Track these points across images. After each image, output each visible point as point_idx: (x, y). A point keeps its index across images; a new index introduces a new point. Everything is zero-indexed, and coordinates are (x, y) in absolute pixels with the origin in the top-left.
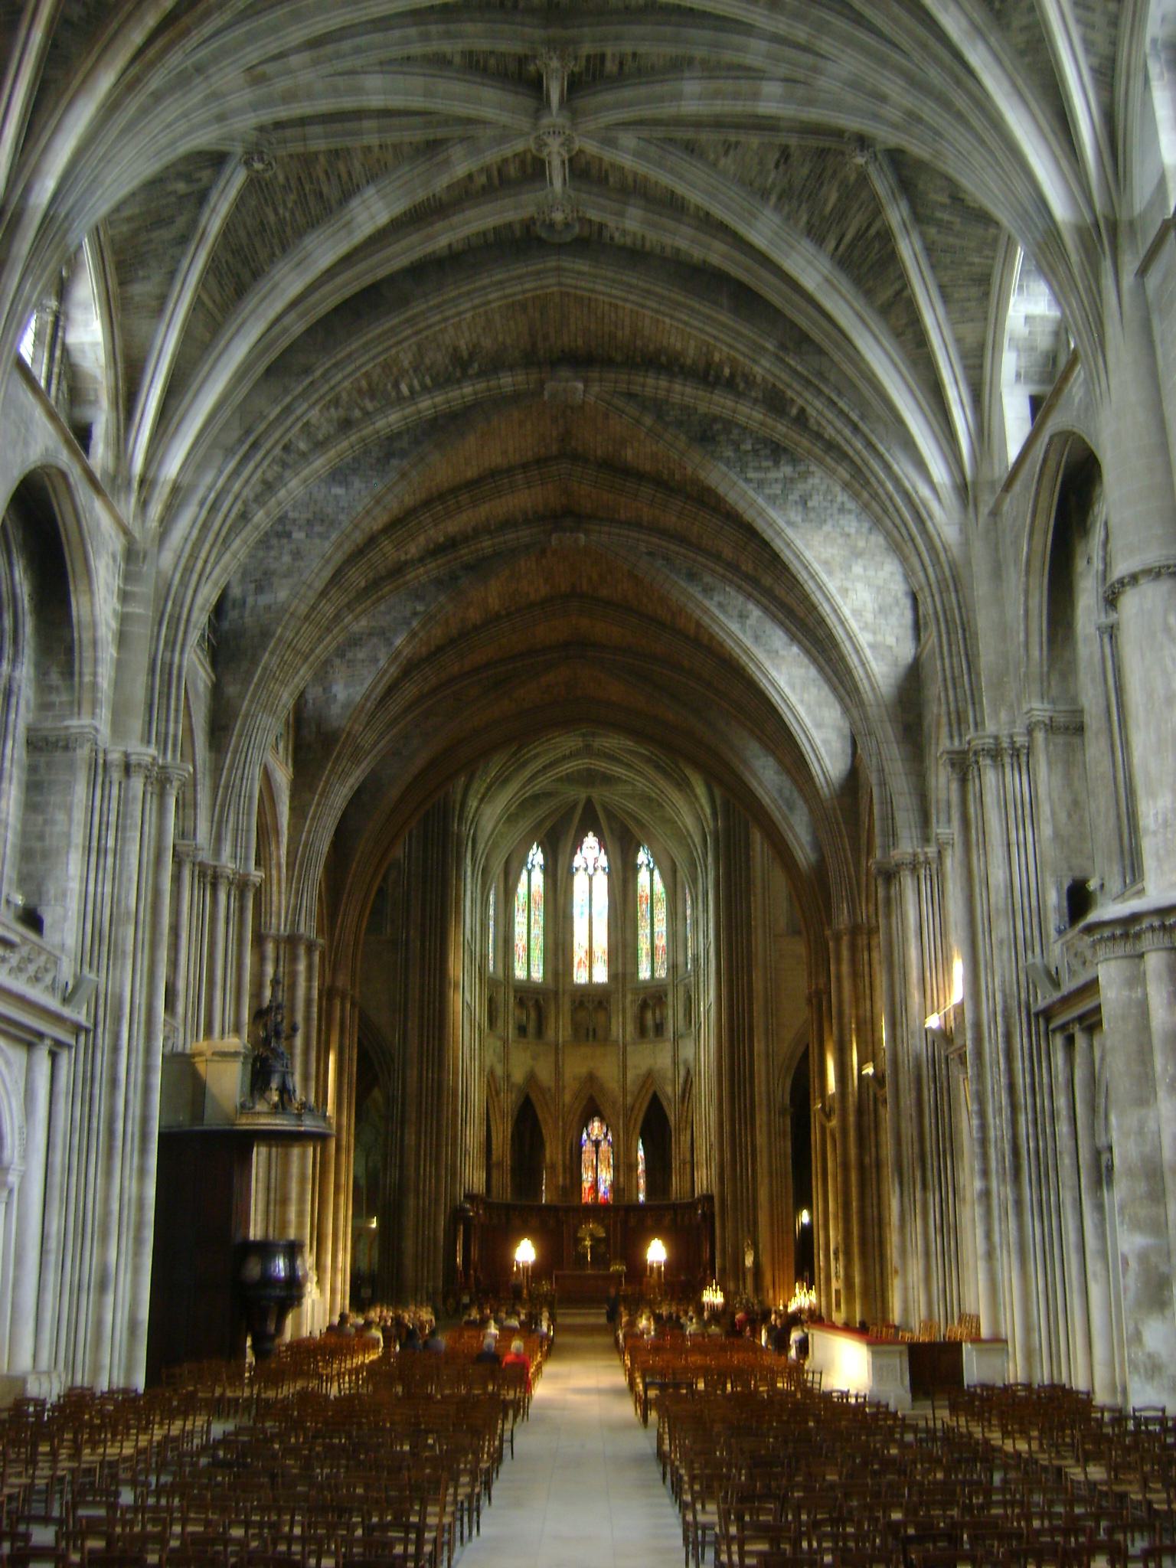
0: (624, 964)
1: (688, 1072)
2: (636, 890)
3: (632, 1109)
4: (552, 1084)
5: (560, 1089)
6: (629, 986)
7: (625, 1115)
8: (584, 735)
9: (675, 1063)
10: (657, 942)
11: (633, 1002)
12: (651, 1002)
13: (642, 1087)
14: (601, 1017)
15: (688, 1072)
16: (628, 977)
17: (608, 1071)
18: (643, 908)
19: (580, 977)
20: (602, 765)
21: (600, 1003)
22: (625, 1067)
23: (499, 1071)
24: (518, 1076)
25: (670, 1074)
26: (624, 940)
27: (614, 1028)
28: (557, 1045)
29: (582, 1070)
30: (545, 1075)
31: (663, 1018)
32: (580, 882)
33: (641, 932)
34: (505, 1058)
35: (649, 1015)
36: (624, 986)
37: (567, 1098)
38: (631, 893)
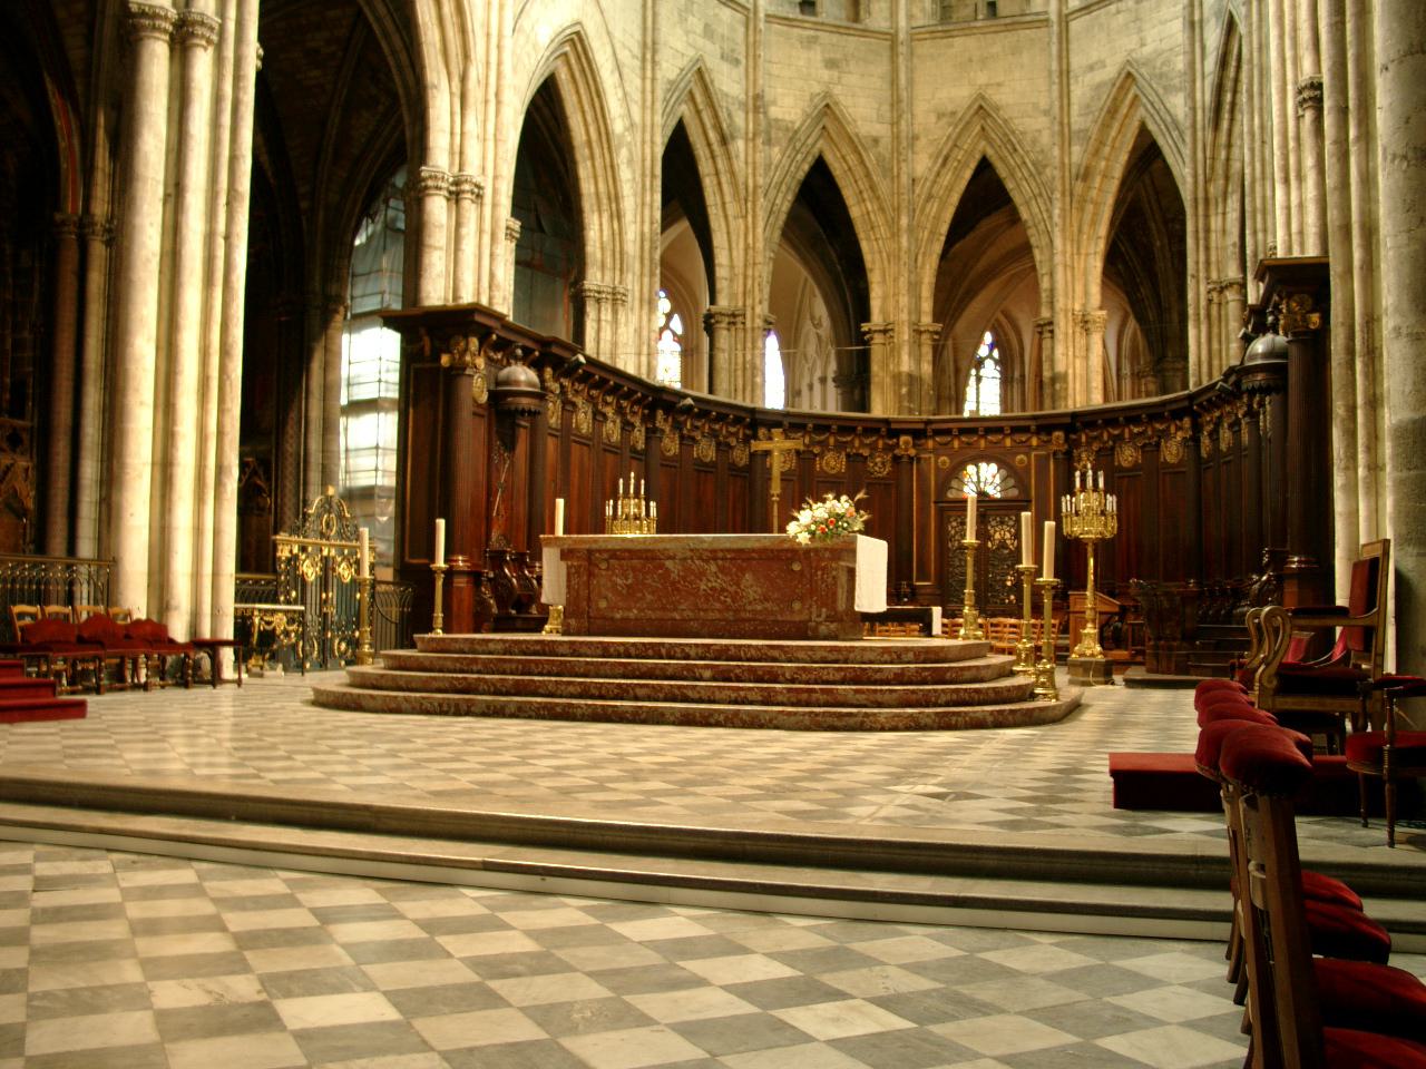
1: (1231, 26)
3: (1086, 175)
4: (882, 130)
5: (903, 143)
9: (1193, 26)
13: (1112, 112)
15: (1231, 26)
22: (1065, 74)
23: (729, 83)
24: (788, 107)
25: (1180, 63)
28: (892, 38)
29: (958, 94)
30: (864, 110)
34: (750, 58)
37: (922, 164)
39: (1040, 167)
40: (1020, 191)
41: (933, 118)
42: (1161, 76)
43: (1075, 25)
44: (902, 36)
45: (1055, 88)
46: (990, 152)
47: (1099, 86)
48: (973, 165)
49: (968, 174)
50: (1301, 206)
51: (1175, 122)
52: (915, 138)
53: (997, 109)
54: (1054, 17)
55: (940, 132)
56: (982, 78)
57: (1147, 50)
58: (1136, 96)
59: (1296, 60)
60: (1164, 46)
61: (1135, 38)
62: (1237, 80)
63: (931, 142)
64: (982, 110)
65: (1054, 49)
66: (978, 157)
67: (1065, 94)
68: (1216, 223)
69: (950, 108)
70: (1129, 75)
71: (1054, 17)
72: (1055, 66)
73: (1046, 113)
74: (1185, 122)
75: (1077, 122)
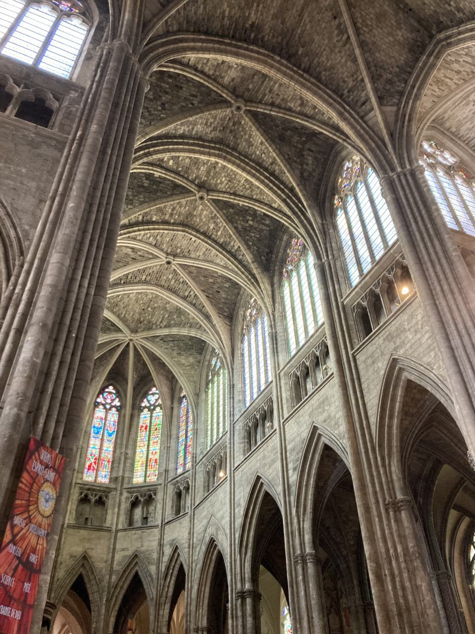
0: (124, 471)
2: (138, 423)
6: (125, 486)
7: (109, 592)
8: (168, 254)
9: (161, 545)
10: (150, 456)
11: (127, 498)
12: (142, 500)
14: (98, 511)
16: (126, 480)
17: (99, 551)
18: (142, 435)
19: (88, 477)
20: (165, 295)
21: (100, 498)
22: (114, 549)
25: (155, 556)
26: (126, 454)
27: (109, 517)
29: (78, 550)
31: (148, 513)
32: (100, 412)
33: (138, 450)
35: (138, 512)
36: (122, 485)
38: (135, 423)
39: (101, 581)
40: (91, 589)
41: (68, 557)
42: (147, 558)
43: (119, 534)
44: (65, 526)
45: (111, 554)
46: (83, 572)
47: (126, 556)
48: (77, 576)
49: (74, 579)
50: (237, 626)
51: (150, 575)
52: (61, 563)
53: (90, 558)
54: (114, 530)
55: (71, 562)
56: (87, 546)
57: (143, 549)
58: (136, 563)
59: (236, 583)
60: (149, 548)
61: (140, 544)
62: (174, 566)
63: (66, 566)
64: (85, 557)
65: (112, 541)
66: (79, 573)
67: (113, 557)
68: (161, 613)
69: (75, 554)
70: (136, 555)
71: (114, 529)
72: (112, 546)
73: (106, 562)
74: (154, 576)
75: (115, 567)
